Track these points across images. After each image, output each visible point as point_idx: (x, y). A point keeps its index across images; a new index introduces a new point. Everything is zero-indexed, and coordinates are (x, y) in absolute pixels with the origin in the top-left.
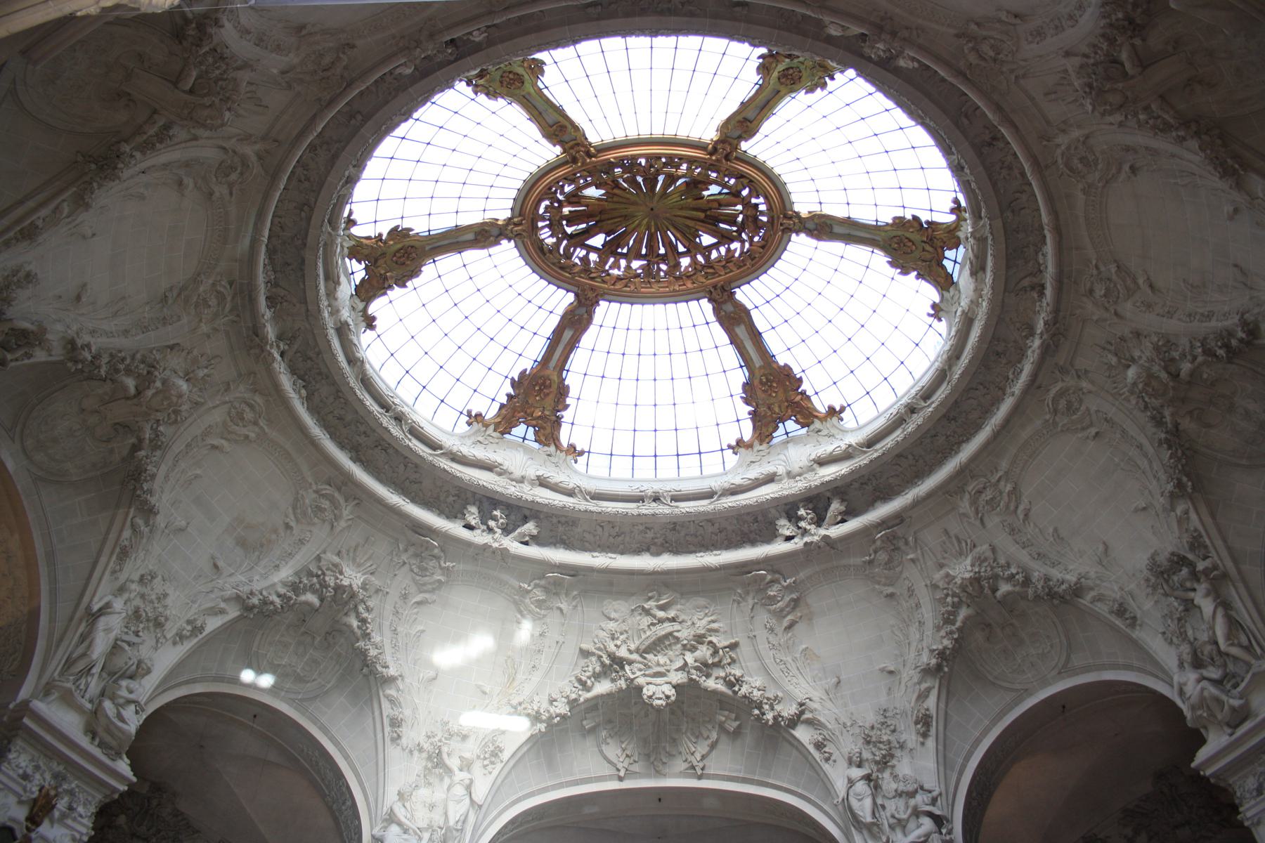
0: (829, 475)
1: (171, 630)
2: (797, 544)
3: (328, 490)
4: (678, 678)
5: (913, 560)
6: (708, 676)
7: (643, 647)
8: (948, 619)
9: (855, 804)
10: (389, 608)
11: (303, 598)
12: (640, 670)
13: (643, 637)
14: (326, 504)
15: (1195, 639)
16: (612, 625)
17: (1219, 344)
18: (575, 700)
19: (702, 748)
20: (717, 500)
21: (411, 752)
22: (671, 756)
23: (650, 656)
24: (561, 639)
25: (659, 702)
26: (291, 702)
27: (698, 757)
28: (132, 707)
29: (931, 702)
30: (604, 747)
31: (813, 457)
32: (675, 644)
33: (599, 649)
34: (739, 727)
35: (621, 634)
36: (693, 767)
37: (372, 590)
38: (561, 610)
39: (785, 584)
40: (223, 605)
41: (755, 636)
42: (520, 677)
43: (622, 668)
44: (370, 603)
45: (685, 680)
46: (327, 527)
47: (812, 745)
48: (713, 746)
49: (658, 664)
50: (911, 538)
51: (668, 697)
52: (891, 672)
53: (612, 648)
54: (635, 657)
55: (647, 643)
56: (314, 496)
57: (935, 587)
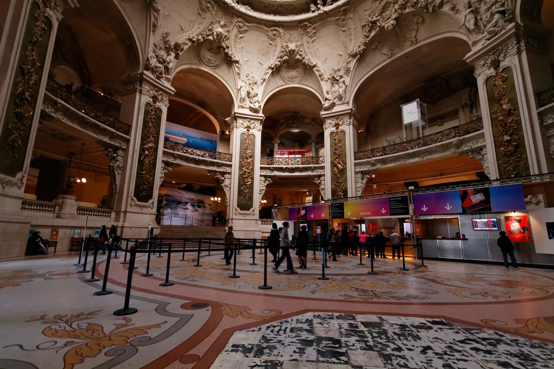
1: (259, 83)
3: (273, 28)
4: (394, 16)
6: (405, 9)
7: (380, 13)
9: (467, 24)
10: (306, 48)
11: (284, 59)
12: (382, 21)
13: (379, 9)
14: (275, 32)
16: (368, 12)
18: (365, 43)
19: (414, 33)
21: (327, 81)
22: (404, 42)
23: (384, 14)
24: (355, 27)
25: (390, 28)
26: (297, 83)
27: (413, 37)
28: (257, 102)
30: (382, 51)
32: (391, 4)
33: (367, 22)
34: (423, 19)
35: (372, 13)
36: (413, 42)
37: (300, 46)
38: (351, 18)
40: (267, 71)
42: (348, 45)
43: (376, 24)
44: (301, 50)
45: (398, 15)
46: (279, 38)
47: (450, 11)
48: (417, 30)
49: (387, 15)
51: (393, 24)
53: (370, 19)
54: (379, 17)
55: (380, 11)
56: (271, 32)
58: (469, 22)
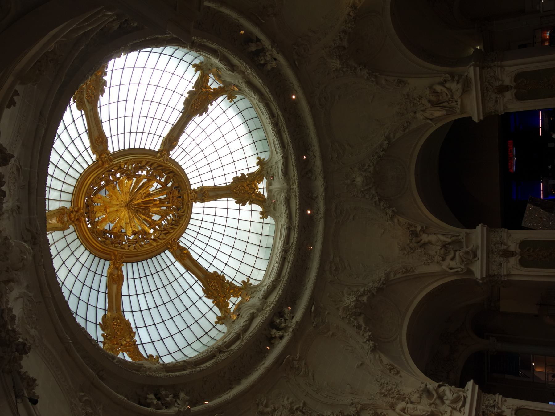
0: (275, 298)
2: (287, 337)
5: (328, 313)
8: (359, 327)
15: (436, 252)
17: (381, 150)
20: (243, 337)
29: (386, 360)
31: (261, 297)
39: (298, 358)
41: (307, 393)
50: (321, 305)
52: (361, 365)
57: (343, 318)
58: (417, 410)
